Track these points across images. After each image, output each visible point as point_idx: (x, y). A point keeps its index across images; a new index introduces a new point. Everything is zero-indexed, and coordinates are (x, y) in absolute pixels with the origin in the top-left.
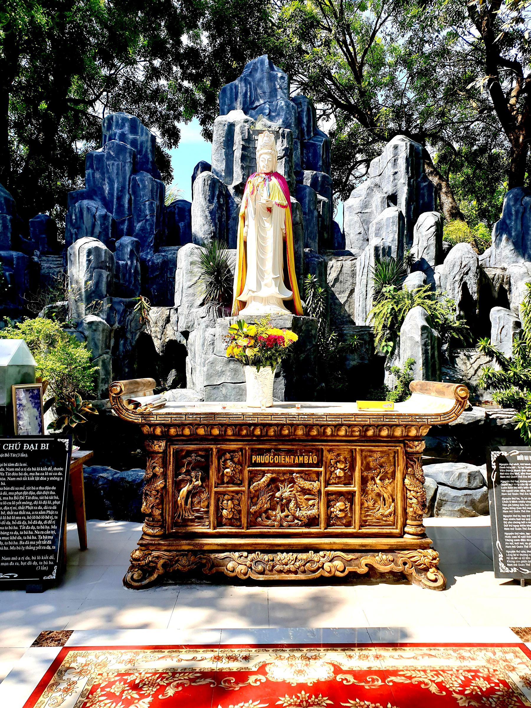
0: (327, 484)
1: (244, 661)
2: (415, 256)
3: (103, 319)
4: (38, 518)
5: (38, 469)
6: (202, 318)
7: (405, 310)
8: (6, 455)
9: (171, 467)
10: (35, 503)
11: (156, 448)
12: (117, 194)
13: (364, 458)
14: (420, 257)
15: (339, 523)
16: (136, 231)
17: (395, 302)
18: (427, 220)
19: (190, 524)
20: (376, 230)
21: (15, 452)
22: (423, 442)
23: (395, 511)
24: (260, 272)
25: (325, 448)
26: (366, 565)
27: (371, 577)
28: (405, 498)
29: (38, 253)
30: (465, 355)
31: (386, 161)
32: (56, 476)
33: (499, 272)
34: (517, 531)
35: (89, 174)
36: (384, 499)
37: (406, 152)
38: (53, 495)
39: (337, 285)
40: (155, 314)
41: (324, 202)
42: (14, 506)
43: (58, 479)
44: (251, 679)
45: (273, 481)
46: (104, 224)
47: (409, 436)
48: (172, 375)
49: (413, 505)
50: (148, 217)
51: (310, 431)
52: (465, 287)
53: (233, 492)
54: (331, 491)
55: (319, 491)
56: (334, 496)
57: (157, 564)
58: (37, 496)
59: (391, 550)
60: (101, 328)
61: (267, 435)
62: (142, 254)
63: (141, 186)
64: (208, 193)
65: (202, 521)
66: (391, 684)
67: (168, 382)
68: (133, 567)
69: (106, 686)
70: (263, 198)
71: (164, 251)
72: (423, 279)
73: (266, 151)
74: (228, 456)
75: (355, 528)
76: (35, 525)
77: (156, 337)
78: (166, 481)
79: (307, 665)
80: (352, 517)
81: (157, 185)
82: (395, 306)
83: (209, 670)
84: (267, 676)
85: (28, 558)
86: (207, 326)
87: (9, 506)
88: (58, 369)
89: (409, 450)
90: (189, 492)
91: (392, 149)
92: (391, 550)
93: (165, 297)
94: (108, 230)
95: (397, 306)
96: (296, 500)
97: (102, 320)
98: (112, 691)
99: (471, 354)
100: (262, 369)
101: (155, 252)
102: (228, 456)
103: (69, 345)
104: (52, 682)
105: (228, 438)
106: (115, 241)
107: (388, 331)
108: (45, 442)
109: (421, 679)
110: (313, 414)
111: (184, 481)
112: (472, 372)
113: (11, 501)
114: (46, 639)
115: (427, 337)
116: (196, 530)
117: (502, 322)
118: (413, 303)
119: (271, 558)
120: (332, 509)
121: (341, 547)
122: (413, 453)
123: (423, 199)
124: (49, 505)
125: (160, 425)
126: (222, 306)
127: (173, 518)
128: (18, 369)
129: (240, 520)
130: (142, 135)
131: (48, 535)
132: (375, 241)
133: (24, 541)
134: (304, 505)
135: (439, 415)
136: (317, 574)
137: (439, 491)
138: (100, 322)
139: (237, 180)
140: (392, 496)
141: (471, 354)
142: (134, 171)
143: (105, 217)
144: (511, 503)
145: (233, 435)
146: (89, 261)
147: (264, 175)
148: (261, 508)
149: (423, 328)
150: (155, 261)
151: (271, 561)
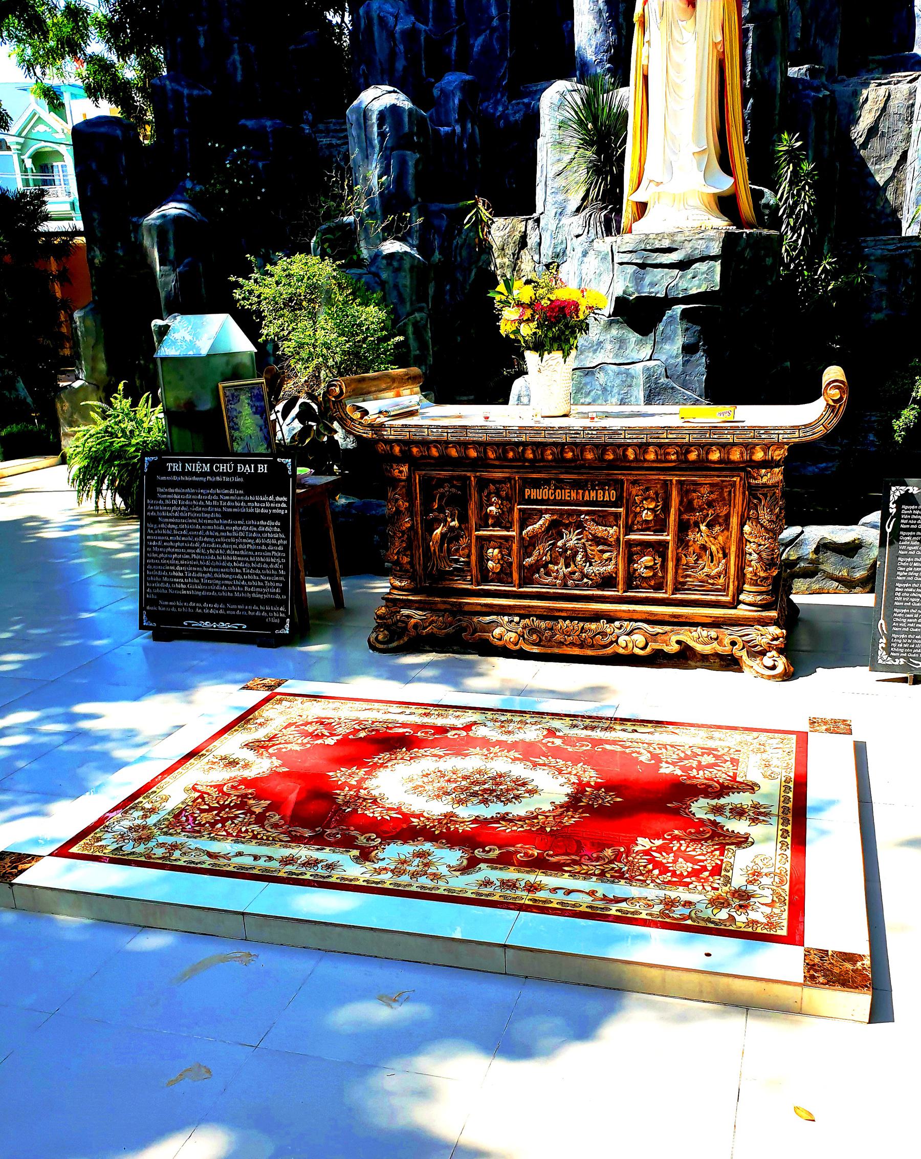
0: (629, 530)
3: (412, 246)
4: (262, 560)
6: (577, 236)
10: (258, 541)
15: (645, 585)
22: (777, 470)
28: (741, 553)
38: (278, 533)
40: (501, 231)
42: (234, 543)
45: (553, 525)
47: (754, 461)
49: (753, 563)
53: (501, 537)
54: (634, 540)
55: (618, 539)
56: (639, 548)
58: (258, 532)
60: (407, 265)
61: (543, 460)
65: (462, 574)
74: (492, 487)
75: (666, 593)
76: (260, 569)
78: (412, 520)
88: (334, 344)
89: (752, 481)
96: (586, 551)
97: (408, 249)
103: (354, 300)
113: (229, 537)
122: (758, 487)
126: (611, 212)
127: (425, 567)
131: (276, 582)
133: (250, 587)
134: (596, 558)
136: (609, 651)
140: (723, 549)
144: (913, 567)
145: (497, 459)
150: (512, 119)
151: (549, 629)
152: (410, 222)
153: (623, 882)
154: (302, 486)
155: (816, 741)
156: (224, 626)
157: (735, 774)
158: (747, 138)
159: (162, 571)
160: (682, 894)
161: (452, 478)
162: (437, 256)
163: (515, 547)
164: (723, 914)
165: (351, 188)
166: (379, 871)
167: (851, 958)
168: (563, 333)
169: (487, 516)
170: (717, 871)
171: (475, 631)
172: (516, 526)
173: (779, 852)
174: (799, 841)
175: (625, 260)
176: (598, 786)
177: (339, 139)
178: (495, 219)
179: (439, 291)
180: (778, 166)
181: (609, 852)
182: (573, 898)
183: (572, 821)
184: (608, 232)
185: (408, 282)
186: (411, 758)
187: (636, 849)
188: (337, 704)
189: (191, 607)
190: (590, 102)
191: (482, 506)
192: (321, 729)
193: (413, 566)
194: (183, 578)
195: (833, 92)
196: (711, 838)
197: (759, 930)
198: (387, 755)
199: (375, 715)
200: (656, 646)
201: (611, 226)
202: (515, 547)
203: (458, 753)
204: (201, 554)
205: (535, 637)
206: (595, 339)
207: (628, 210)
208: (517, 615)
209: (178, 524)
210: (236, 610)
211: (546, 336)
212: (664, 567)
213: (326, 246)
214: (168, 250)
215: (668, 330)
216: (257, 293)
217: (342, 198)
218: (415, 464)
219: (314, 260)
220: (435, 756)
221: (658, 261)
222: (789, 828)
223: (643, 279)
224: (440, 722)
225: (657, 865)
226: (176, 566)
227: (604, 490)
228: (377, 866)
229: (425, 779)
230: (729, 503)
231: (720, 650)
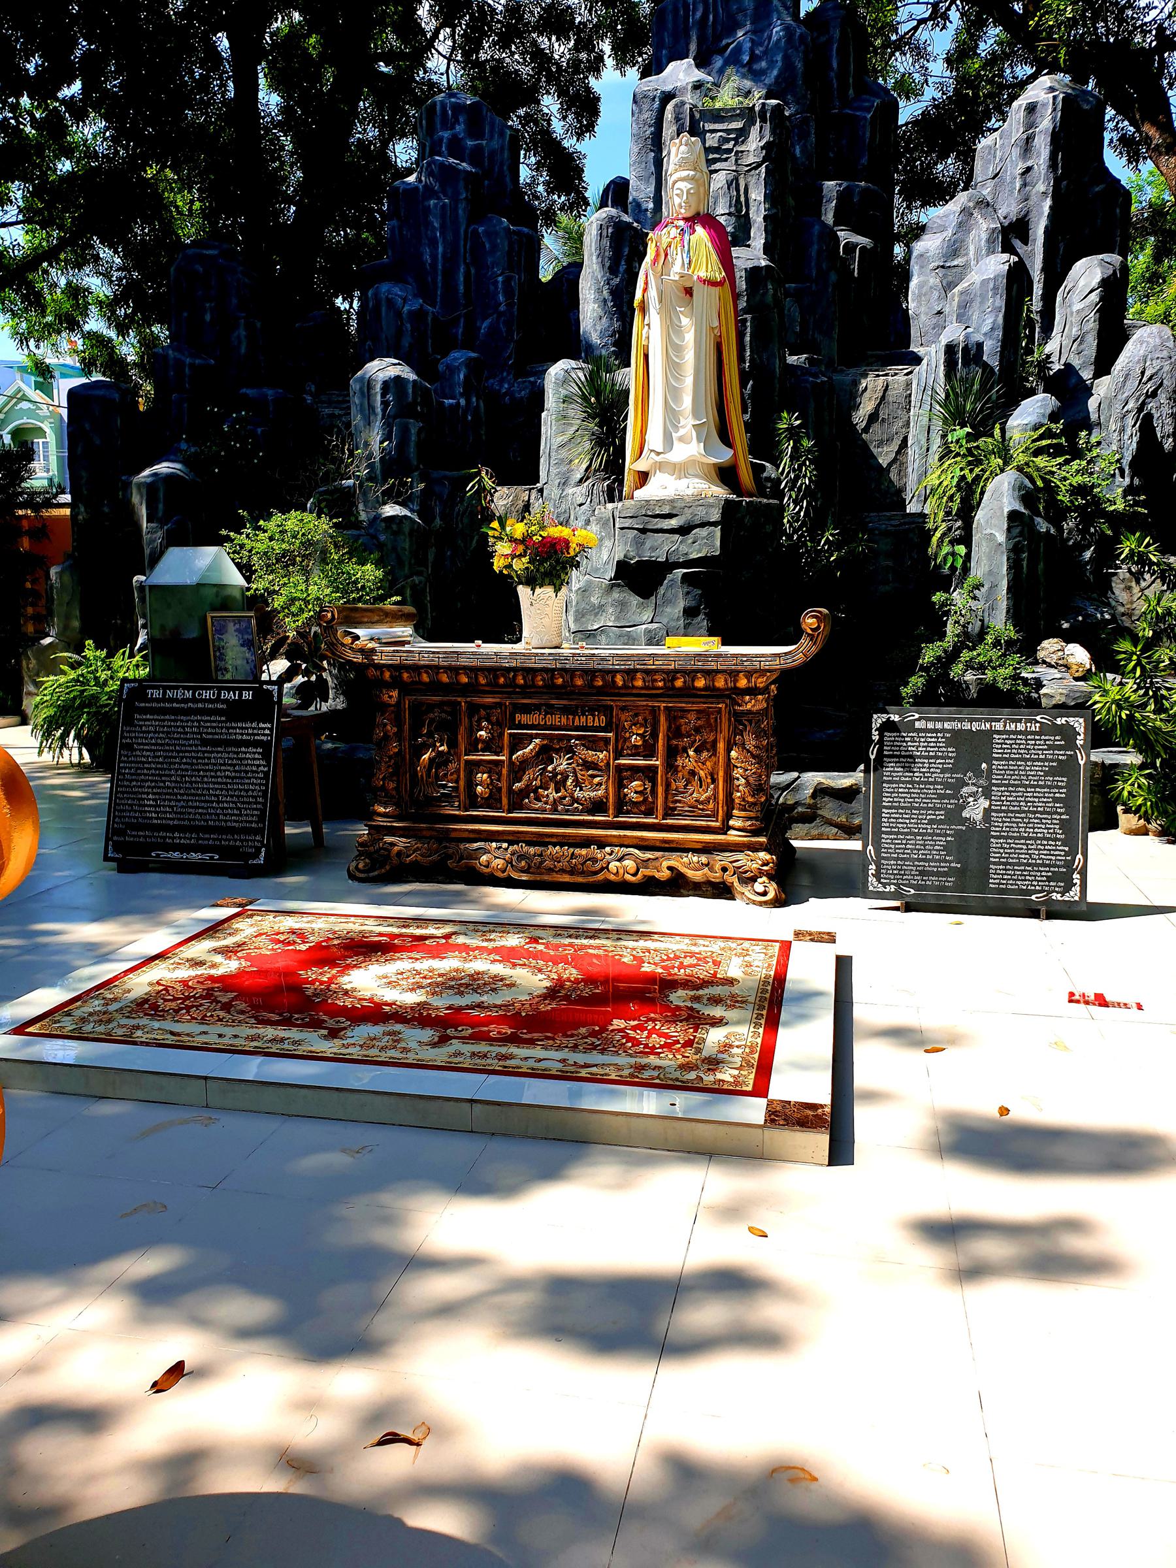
0: (618, 754)
2: (1054, 358)
3: (412, 511)
6: (580, 505)
7: (987, 479)
8: (200, 705)
9: (407, 726)
11: (386, 698)
14: (1062, 362)
15: (635, 810)
18: (1087, 274)
20: (959, 307)
21: (210, 701)
22: (760, 697)
24: (671, 416)
26: (669, 868)
27: (677, 886)
28: (729, 779)
34: (902, 834)
36: (700, 779)
37: (1054, 119)
39: (876, 427)
40: (503, 498)
41: (863, 249)
42: (211, 771)
43: (265, 738)
51: (593, 679)
55: (608, 764)
57: (389, 851)
59: (707, 849)
61: (534, 686)
68: (361, 854)
72: (1049, 411)
73: (685, 173)
74: (483, 712)
76: (238, 797)
78: (400, 745)
80: (653, 803)
82: (967, 472)
85: (229, 837)
87: (205, 771)
92: (707, 849)
93: (522, 468)
95: (971, 471)
96: (576, 776)
103: (350, 559)
107: (959, 523)
108: (248, 689)
111: (423, 748)
113: (207, 764)
115: (1021, 534)
121: (635, 842)
122: (744, 713)
125: (389, 667)
126: (614, 482)
128: (215, 590)
130: (492, 137)
132: (953, 333)
133: (226, 815)
136: (600, 877)
138: (405, 516)
140: (712, 775)
142: (476, 216)
143: (418, 316)
145: (487, 685)
146: (385, 404)
147: (681, 223)
148: (527, 786)
149: (1013, 516)
150: (517, 395)
153: (595, 1052)
154: (288, 716)
155: (796, 947)
156: (195, 856)
157: (716, 973)
158: (747, 417)
159: (133, 799)
160: (652, 1060)
161: (442, 703)
162: (438, 521)
163: (505, 771)
164: (692, 1075)
165: (351, 455)
166: (347, 1046)
167: (813, 1107)
168: (555, 568)
169: (478, 740)
170: (689, 1043)
171: (461, 858)
173: (752, 1029)
174: (772, 1024)
175: (627, 525)
176: (577, 981)
177: (341, 409)
180: (779, 442)
181: (583, 1030)
182: (543, 1065)
183: (549, 1008)
184: (611, 500)
185: (407, 546)
187: (611, 1028)
188: (311, 918)
189: (161, 837)
190: (593, 379)
191: (472, 731)
192: (293, 937)
194: (155, 806)
195: (830, 378)
196: (687, 1020)
197: (725, 1087)
198: (361, 958)
199: (355, 927)
200: (648, 872)
201: (612, 495)
202: (505, 771)
203: (434, 957)
204: (176, 782)
205: (523, 863)
207: (629, 479)
208: (505, 841)
209: (154, 751)
210: (208, 839)
211: (538, 570)
212: (654, 792)
213: (323, 505)
214: (157, 508)
215: (669, 594)
216: (248, 547)
217: (342, 461)
219: (308, 517)
221: (659, 526)
222: (764, 1012)
223: (643, 544)
224: (419, 932)
225: (629, 1039)
226: (148, 794)
227: (594, 716)
228: (345, 1042)
229: (400, 977)
230: (714, 728)
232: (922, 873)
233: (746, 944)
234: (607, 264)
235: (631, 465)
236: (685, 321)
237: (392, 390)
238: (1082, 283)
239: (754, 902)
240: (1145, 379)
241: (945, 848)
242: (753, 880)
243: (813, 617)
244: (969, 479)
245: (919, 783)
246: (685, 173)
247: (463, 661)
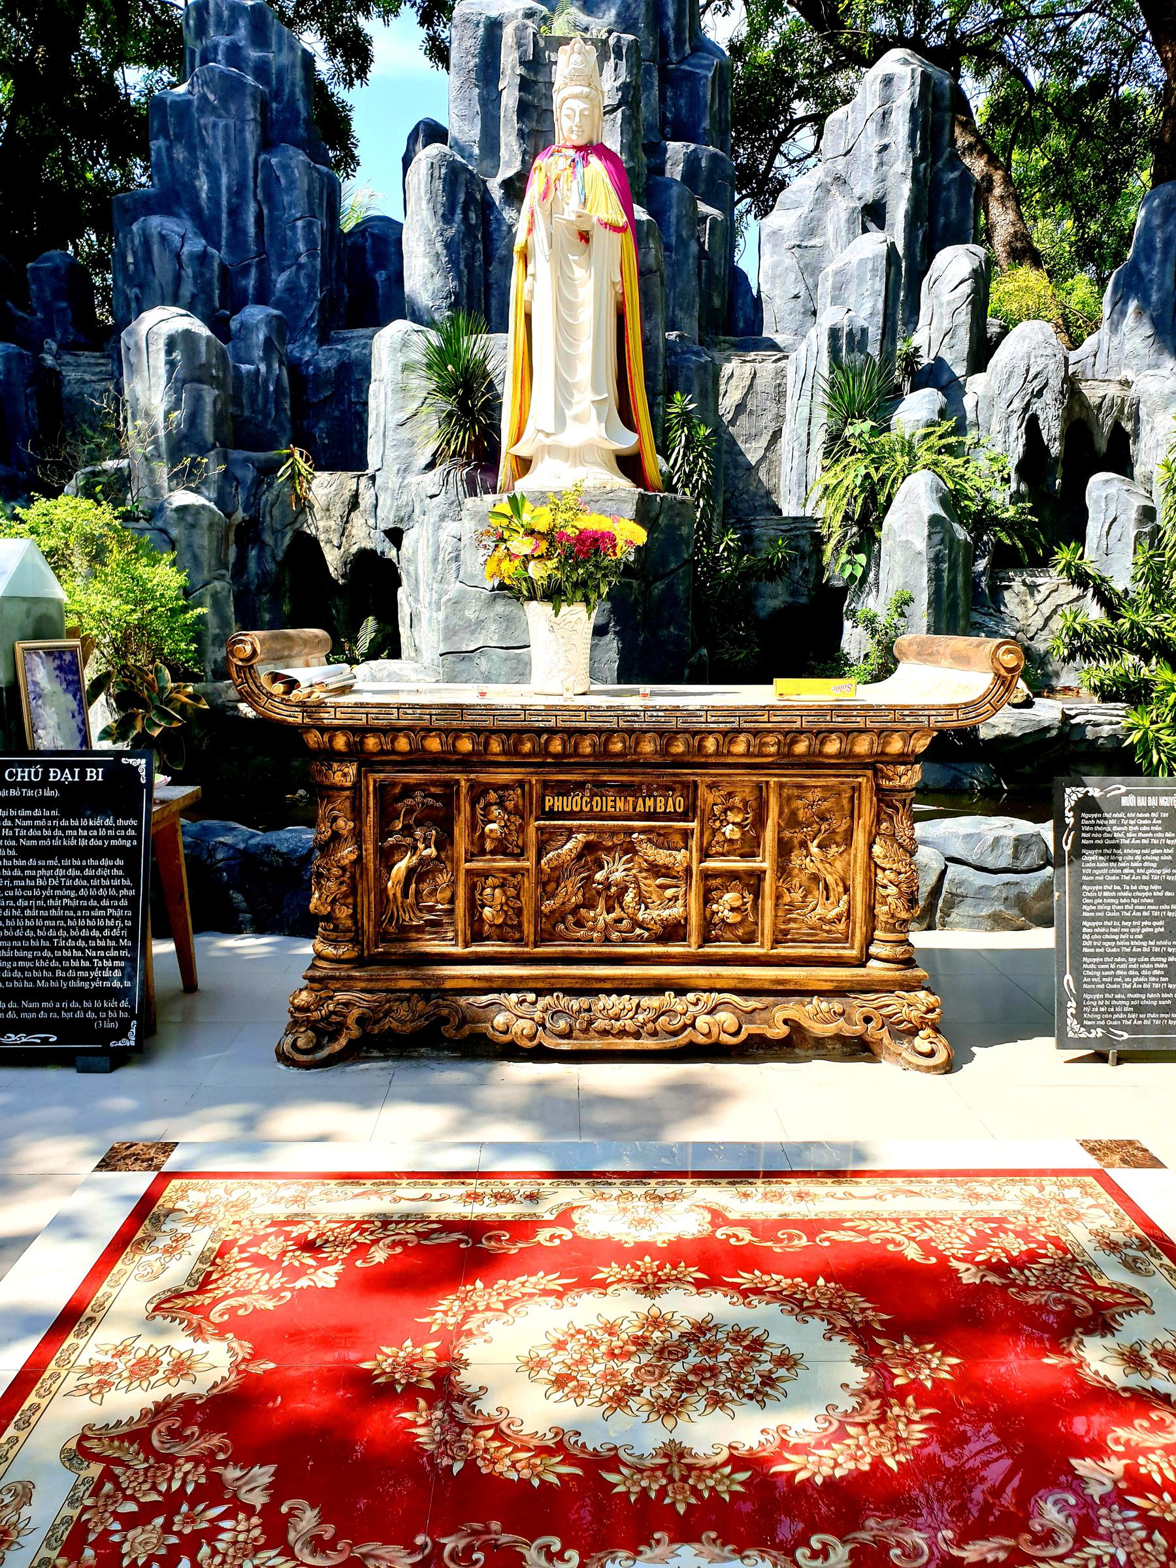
0: (705, 855)
1: (528, 1202)
4: (89, 923)
5: (84, 823)
6: (432, 497)
9: (370, 819)
10: (82, 892)
11: (337, 778)
12: (229, 202)
13: (785, 801)
14: (932, 356)
15: (728, 935)
16: (278, 294)
17: (873, 461)
18: (954, 264)
19: (413, 935)
20: (834, 288)
21: (30, 785)
23: (849, 911)
24: (564, 389)
25: (702, 778)
26: (786, 1022)
27: (793, 1045)
28: (872, 885)
29: (54, 346)
30: (1024, 583)
31: (861, 117)
32: (123, 838)
33: (1113, 390)
35: (159, 148)
38: (119, 877)
39: (743, 419)
40: (325, 488)
41: (714, 220)
42: (38, 898)
44: (543, 1236)
45: (589, 848)
46: (202, 275)
48: (368, 629)
49: (889, 899)
50: (303, 259)
51: (668, 745)
52: (1032, 427)
53: (504, 870)
54: (713, 869)
55: (688, 870)
56: (719, 880)
57: (345, 1017)
58: (84, 878)
59: (839, 992)
60: (205, 520)
61: (576, 753)
62: (293, 349)
63: (283, 181)
64: (441, 199)
66: (827, 1244)
67: (360, 644)
68: (296, 1023)
69: (250, 1244)
70: (570, 210)
71: (343, 341)
72: (937, 408)
73: (578, 90)
75: (762, 946)
76: (86, 939)
77: (329, 541)
78: (360, 848)
79: (656, 1209)
81: (321, 179)
82: (872, 471)
83: (457, 1218)
84: (576, 1230)
85: (74, 1005)
86: (443, 518)
87: (28, 898)
88: (116, 613)
89: (885, 783)
90: (411, 871)
91: (877, 86)
92: (839, 992)
93: (345, 449)
94: (213, 290)
95: (877, 469)
97: (207, 503)
98: (262, 1252)
99: (1039, 581)
100: (564, 608)
101: (321, 343)
102: (493, 796)
103: (137, 559)
104: (140, 1234)
105: (493, 758)
106: (228, 318)
107: (855, 529)
109: (888, 1236)
110: (677, 709)
112: (1038, 621)
113: (31, 888)
114: (124, 1158)
115: (942, 541)
116: (428, 950)
117: (1112, 508)
118: (912, 465)
119: (586, 1006)
120: (715, 907)
122: (893, 790)
123: (947, 215)
124: (111, 898)
126: (476, 468)
127: (379, 923)
128: (24, 606)
129: (519, 927)
130: (280, 50)
131: (113, 959)
132: (830, 316)
133: (66, 969)
134: (654, 897)
135: (955, 707)
136: (682, 1040)
137: (948, 876)
138: (203, 507)
139: (508, 164)
140: (843, 880)
141: (1039, 581)
142: (267, 144)
143: (202, 259)
145: (504, 753)
146: (171, 364)
147: (572, 152)
149: (934, 521)
150: (323, 365)
152: (207, 469)
171: (464, 1021)
172: (532, 853)
177: (94, 374)
178: (317, 474)
179: (242, 558)
186: (507, 1304)
193: (355, 922)
206: (473, 617)
208: (531, 990)
210: (37, 1011)
218: (367, 762)
220: (546, 1293)
227: (667, 798)
231: (849, 1030)
232: (1138, 1009)
233: (1050, 1186)
234: (441, 212)
235: (508, 449)
236: (579, 273)
237: (180, 345)
238: (949, 273)
239: (918, 1068)
240: (1030, 377)
241: (1167, 973)
242: (913, 1032)
243: (1009, 651)
244: (876, 477)
245: (1129, 883)
246: (578, 90)
247: (469, 721)
